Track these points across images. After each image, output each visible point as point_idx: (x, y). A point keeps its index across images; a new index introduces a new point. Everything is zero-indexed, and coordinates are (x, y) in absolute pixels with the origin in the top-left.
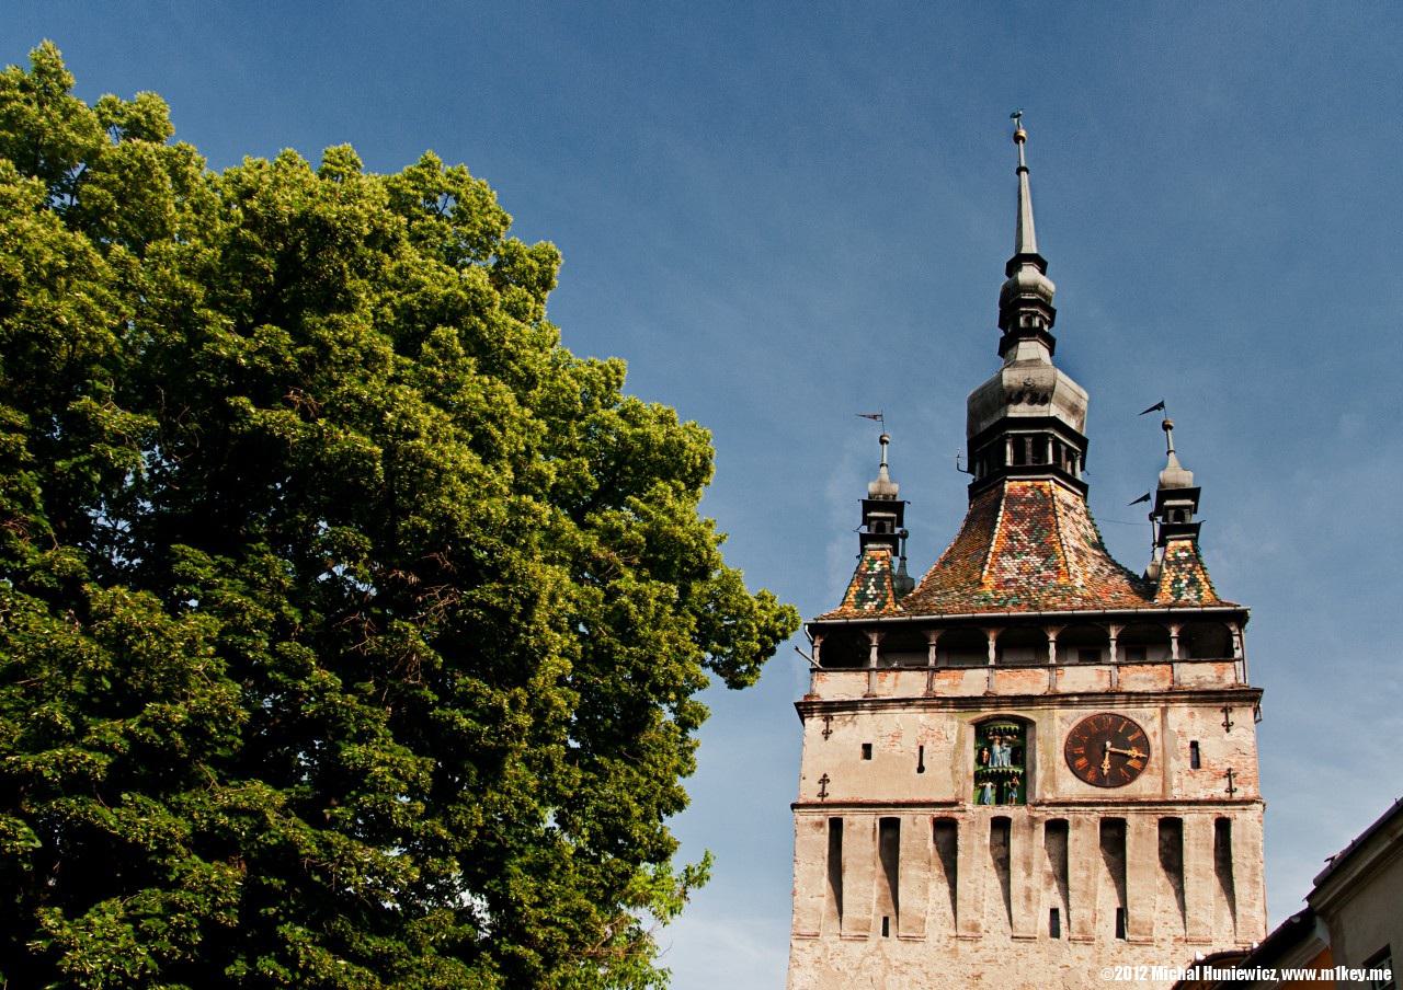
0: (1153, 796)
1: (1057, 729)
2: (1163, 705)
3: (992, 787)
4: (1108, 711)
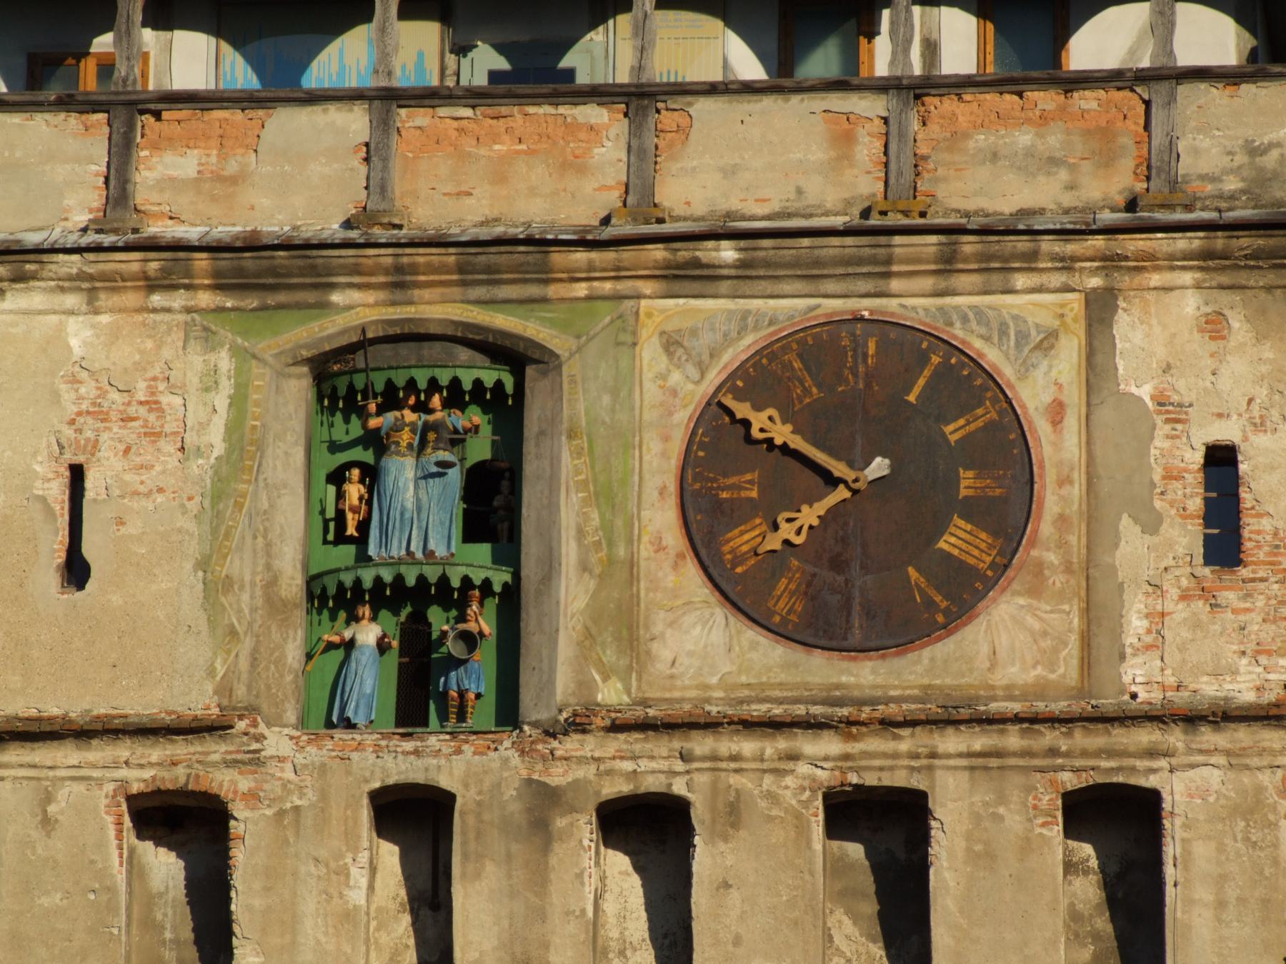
0: (1040, 689)
1: (651, 391)
2: (1095, 282)
3: (382, 647)
4: (865, 307)
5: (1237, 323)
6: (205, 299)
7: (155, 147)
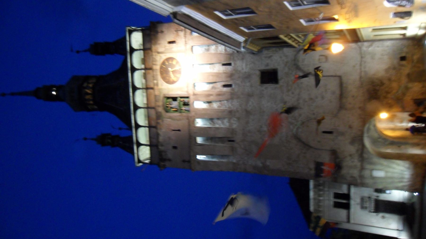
3: (185, 107)
5: (159, 42)
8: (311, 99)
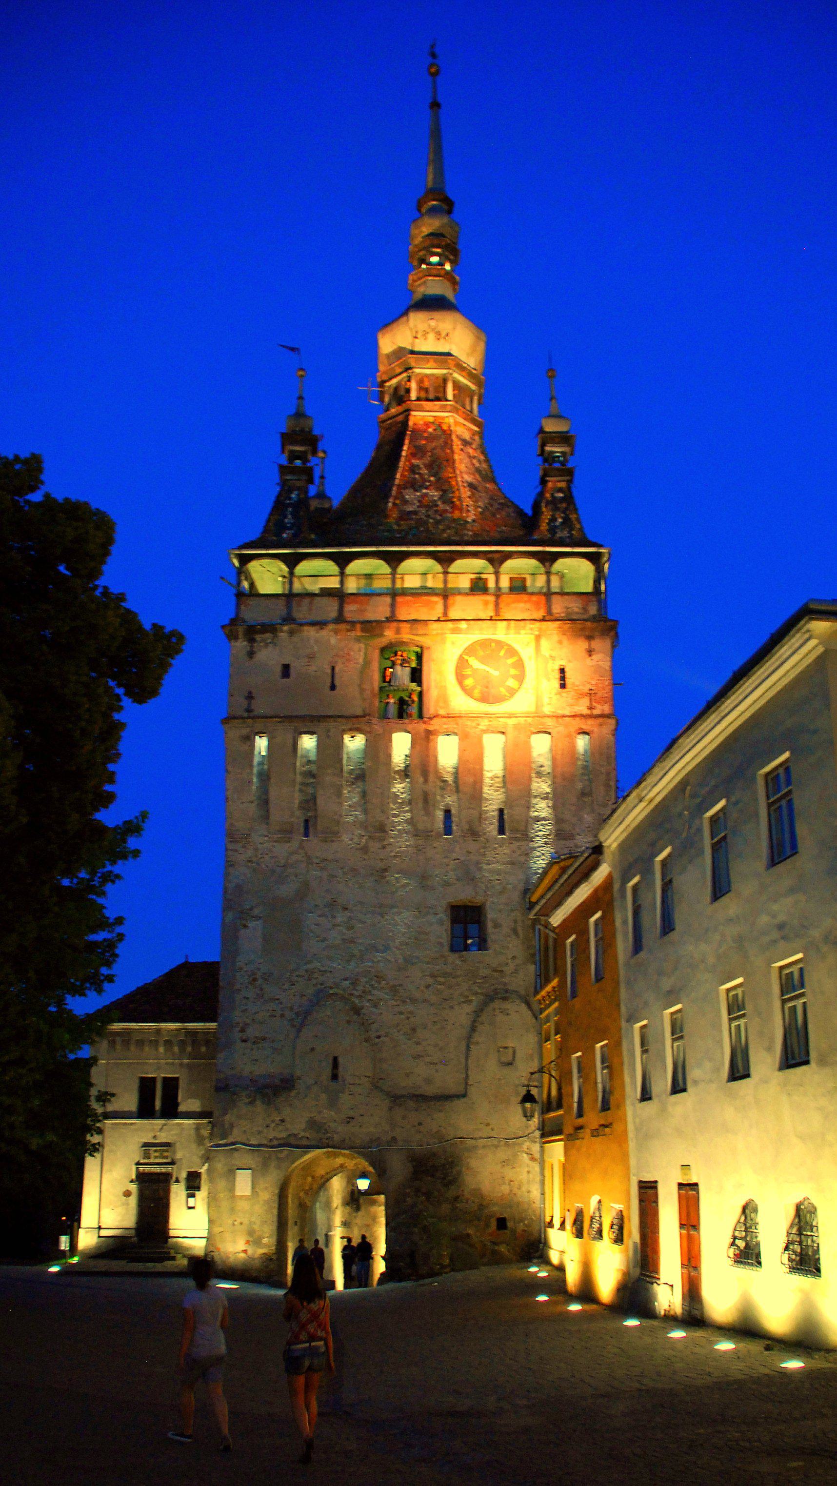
2: (537, 633)
5: (565, 642)
6: (359, 634)
7: (349, 603)
8: (414, 1030)
